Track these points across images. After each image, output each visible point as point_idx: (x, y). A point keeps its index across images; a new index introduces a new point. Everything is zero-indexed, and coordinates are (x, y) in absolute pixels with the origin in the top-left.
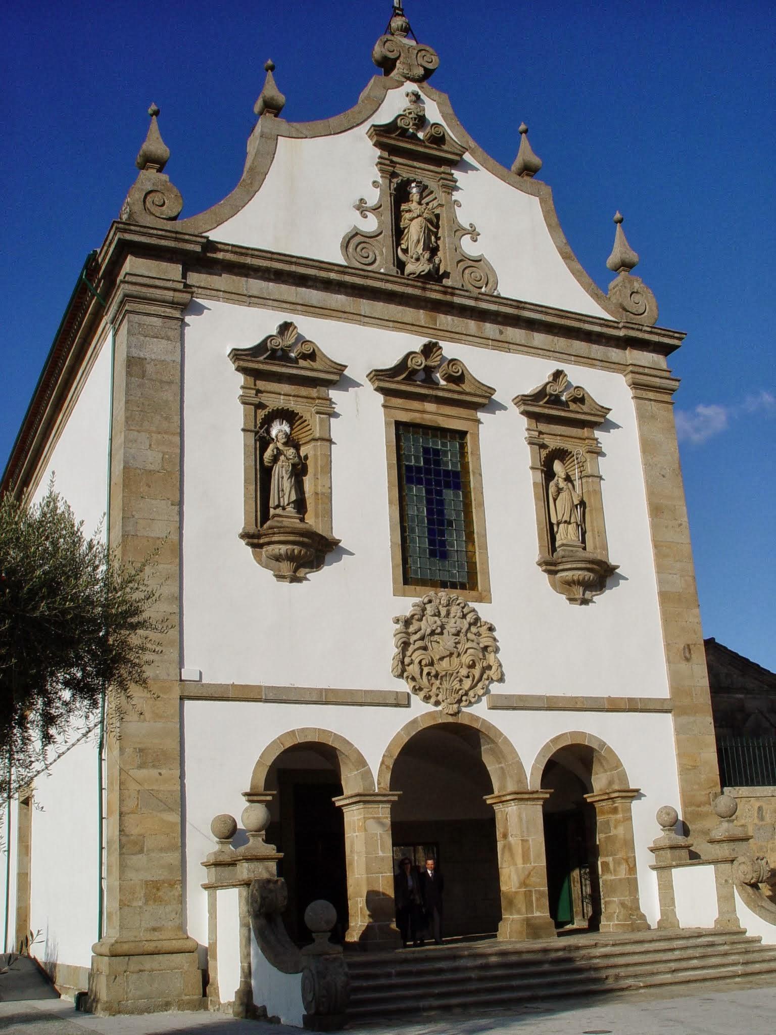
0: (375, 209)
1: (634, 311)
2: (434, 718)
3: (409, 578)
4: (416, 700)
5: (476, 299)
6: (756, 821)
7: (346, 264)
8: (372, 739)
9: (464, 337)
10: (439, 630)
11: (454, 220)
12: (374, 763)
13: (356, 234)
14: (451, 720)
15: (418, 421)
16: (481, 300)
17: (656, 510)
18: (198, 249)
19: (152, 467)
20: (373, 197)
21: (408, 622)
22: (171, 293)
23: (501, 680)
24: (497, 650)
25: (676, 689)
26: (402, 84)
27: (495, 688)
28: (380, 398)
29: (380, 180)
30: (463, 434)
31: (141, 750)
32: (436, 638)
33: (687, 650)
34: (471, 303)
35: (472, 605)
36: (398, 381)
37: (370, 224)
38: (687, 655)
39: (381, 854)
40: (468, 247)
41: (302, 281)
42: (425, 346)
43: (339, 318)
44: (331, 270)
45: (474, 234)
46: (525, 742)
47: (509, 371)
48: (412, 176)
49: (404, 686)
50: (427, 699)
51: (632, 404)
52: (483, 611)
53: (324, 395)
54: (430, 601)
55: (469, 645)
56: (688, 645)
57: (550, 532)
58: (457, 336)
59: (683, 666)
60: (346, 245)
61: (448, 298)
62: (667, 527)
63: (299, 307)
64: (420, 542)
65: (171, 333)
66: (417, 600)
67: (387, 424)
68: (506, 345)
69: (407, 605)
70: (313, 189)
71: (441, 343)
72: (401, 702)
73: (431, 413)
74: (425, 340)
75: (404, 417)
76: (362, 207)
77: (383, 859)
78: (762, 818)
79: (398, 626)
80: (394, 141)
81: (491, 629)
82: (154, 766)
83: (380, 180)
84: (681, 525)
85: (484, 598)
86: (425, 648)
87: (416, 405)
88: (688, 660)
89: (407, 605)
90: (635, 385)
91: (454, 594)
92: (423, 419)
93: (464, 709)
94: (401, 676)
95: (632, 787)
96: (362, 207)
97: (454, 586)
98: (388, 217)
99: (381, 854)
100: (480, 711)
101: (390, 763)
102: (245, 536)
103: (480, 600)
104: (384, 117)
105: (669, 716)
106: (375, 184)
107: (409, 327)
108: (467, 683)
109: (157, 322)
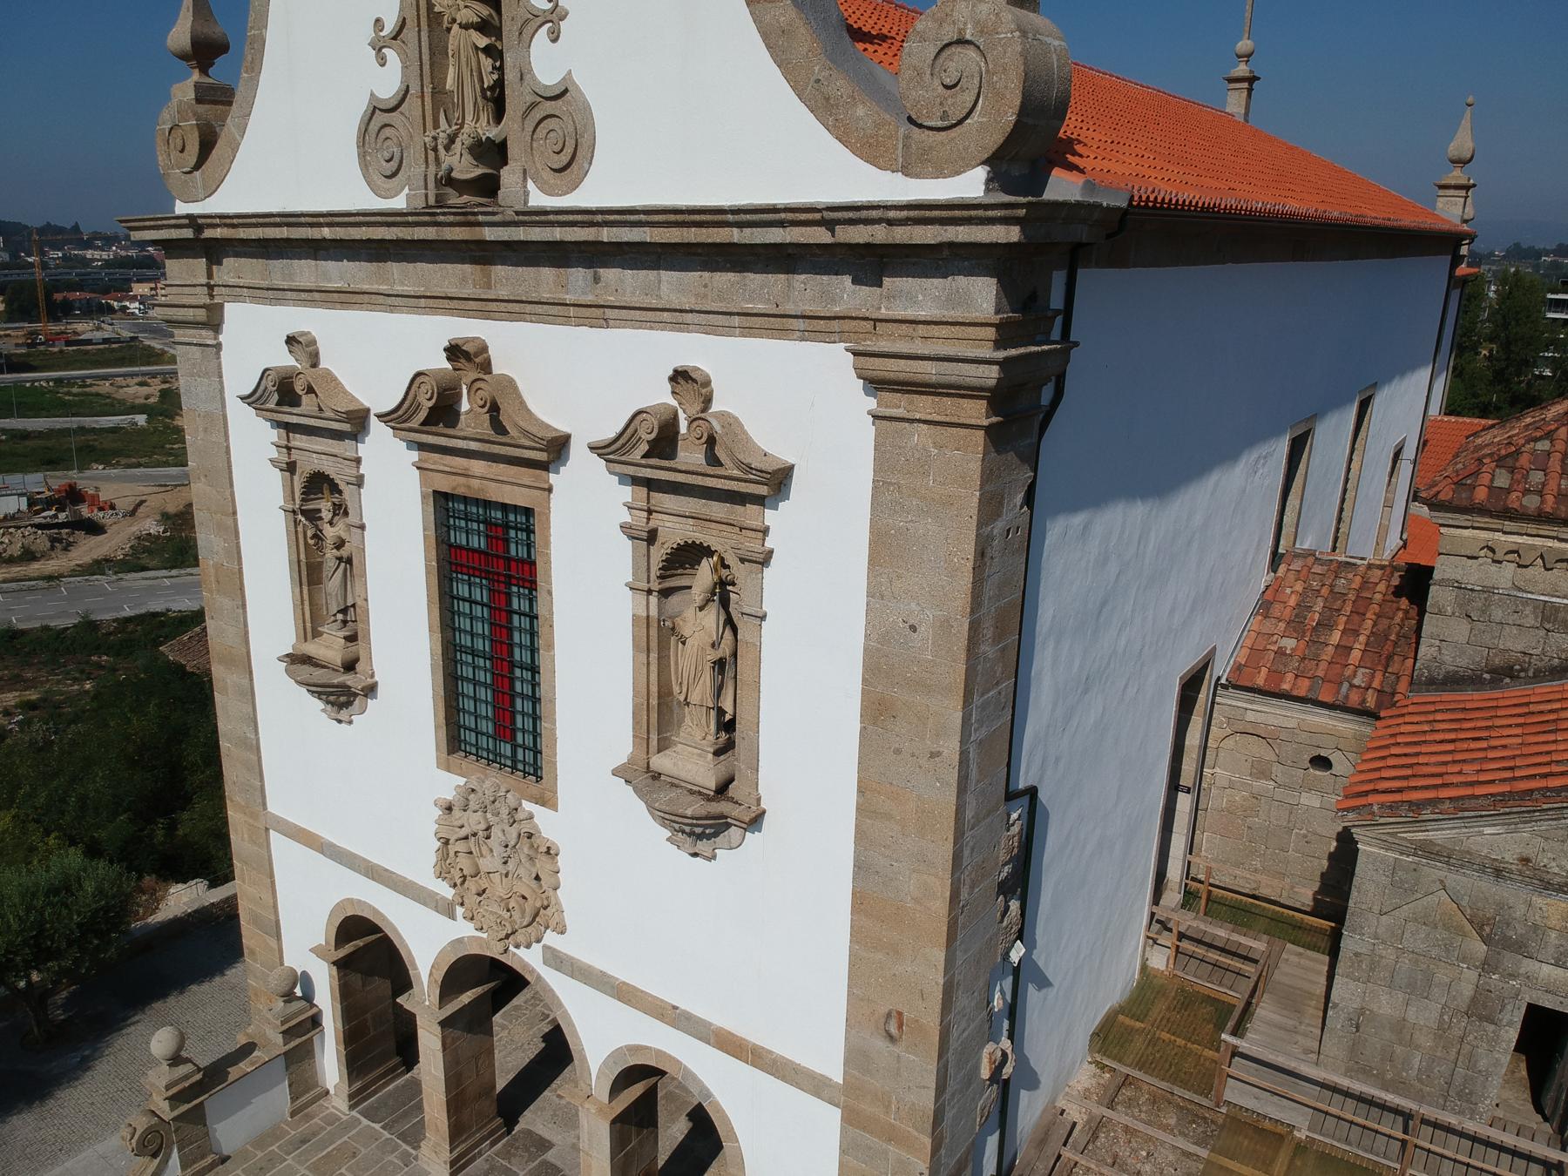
9: (529, 308)
17: (877, 711)
27: (550, 938)
30: (528, 512)
35: (527, 806)
51: (868, 431)
53: (349, 454)
59: (881, 1044)
62: (898, 751)
67: (424, 497)
68: (599, 312)
75: (445, 484)
84: (939, 754)
88: (891, 1037)
89: (449, 784)
92: (469, 487)
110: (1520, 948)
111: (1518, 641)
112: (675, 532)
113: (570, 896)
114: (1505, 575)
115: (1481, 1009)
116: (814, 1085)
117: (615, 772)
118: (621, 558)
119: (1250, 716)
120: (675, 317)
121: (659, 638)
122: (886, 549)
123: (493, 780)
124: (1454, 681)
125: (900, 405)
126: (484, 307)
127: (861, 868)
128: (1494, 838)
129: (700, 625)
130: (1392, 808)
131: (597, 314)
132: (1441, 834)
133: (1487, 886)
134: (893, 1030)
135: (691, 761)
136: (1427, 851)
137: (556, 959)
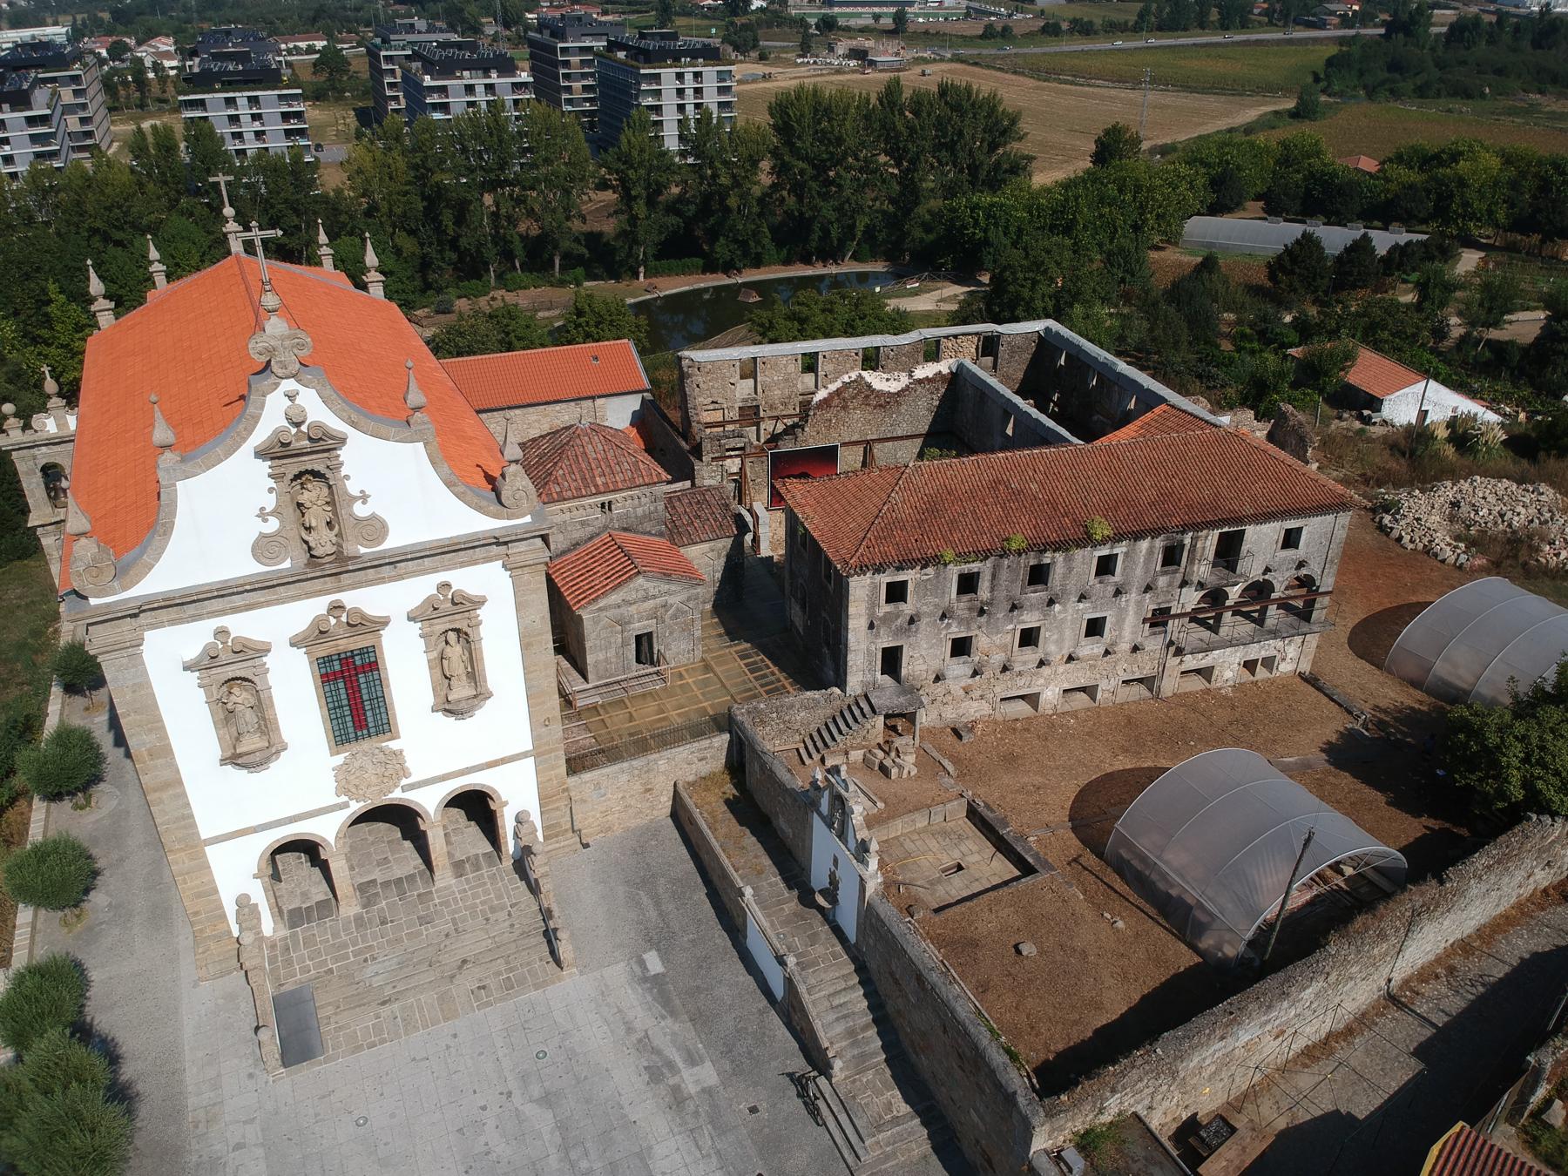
0: (274, 513)
11: (346, 492)
12: (332, 842)
13: (263, 536)
17: (525, 646)
20: (270, 502)
27: (404, 782)
37: (273, 525)
40: (360, 510)
45: (364, 498)
48: (303, 469)
49: (344, 799)
52: (393, 745)
69: (340, 759)
70: (220, 513)
72: (345, 805)
76: (263, 515)
80: (276, 452)
85: (396, 737)
89: (340, 759)
96: (263, 515)
98: (290, 511)
102: (223, 761)
104: (261, 434)
106: (271, 490)
109: (125, 661)
110: (629, 623)
111: (578, 534)
113: (410, 763)
114: (567, 516)
115: (624, 644)
116: (524, 755)
120: (435, 570)
121: (440, 664)
122: (520, 607)
123: (366, 745)
124: (564, 553)
125: (519, 572)
126: (340, 589)
128: (614, 598)
129: (456, 651)
130: (589, 603)
131: (400, 577)
132: (602, 603)
133: (618, 611)
135: (461, 691)
136: (600, 609)
137: (412, 787)
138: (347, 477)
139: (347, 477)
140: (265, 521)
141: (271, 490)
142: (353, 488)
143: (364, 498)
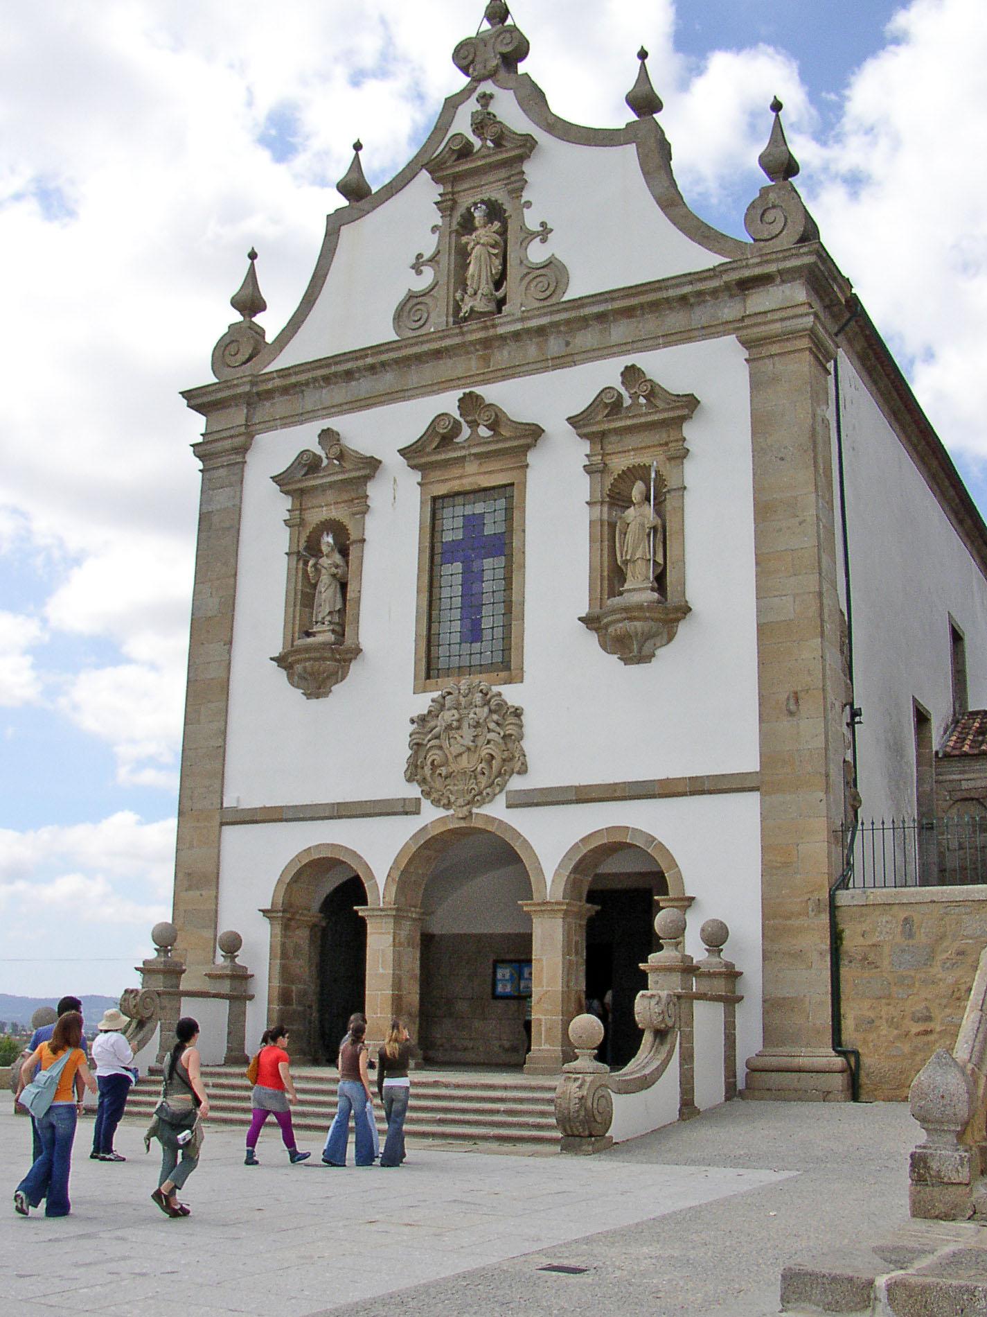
1: (766, 236)
2: (445, 823)
3: (430, 668)
4: (426, 804)
5: (522, 319)
6: (899, 939)
7: (398, 338)
8: (379, 850)
10: (455, 723)
11: (522, 227)
13: (411, 296)
14: (463, 824)
15: (457, 489)
16: (529, 318)
18: (247, 388)
19: (210, 614)
21: (422, 720)
22: (230, 441)
23: (523, 771)
24: (521, 737)
25: (768, 757)
26: (475, 88)
28: (417, 476)
29: (439, 222)
31: (189, 874)
32: (453, 733)
33: (792, 701)
34: (519, 326)
35: (495, 689)
36: (432, 451)
38: (793, 707)
39: (381, 971)
40: (537, 253)
41: (349, 375)
42: (460, 400)
43: (382, 403)
44: (366, 356)
46: (552, 843)
47: (548, 397)
48: (478, 198)
49: (414, 791)
50: (436, 803)
52: (511, 694)
54: (449, 693)
55: (491, 736)
56: (796, 693)
57: (612, 576)
58: (509, 372)
60: (398, 317)
61: (491, 332)
63: (346, 407)
64: (452, 627)
65: (234, 478)
66: (436, 694)
71: (478, 390)
72: (408, 808)
73: (475, 476)
74: (459, 393)
75: (441, 490)
77: (382, 976)
78: (911, 936)
79: (415, 725)
81: (518, 713)
82: (198, 889)
83: (439, 222)
86: (440, 748)
87: (456, 472)
88: (791, 713)
89: (422, 704)
90: (747, 344)
91: (475, 679)
93: (475, 810)
94: (409, 780)
95: (688, 894)
96: (417, 268)
97: (483, 669)
98: (445, 261)
99: (381, 971)
100: (496, 809)
101: (396, 875)
103: (509, 681)
105: (755, 797)
107: (455, 383)
108: (484, 781)
112: (620, 464)
117: (580, 619)
118: (582, 487)
119: (965, 785)
127: (759, 611)
134: (793, 707)
138: (528, 204)
139: (528, 204)
140: (419, 273)
141: (435, 229)
142: (532, 221)
143: (545, 232)
